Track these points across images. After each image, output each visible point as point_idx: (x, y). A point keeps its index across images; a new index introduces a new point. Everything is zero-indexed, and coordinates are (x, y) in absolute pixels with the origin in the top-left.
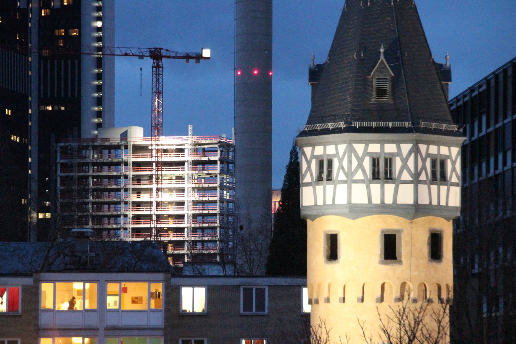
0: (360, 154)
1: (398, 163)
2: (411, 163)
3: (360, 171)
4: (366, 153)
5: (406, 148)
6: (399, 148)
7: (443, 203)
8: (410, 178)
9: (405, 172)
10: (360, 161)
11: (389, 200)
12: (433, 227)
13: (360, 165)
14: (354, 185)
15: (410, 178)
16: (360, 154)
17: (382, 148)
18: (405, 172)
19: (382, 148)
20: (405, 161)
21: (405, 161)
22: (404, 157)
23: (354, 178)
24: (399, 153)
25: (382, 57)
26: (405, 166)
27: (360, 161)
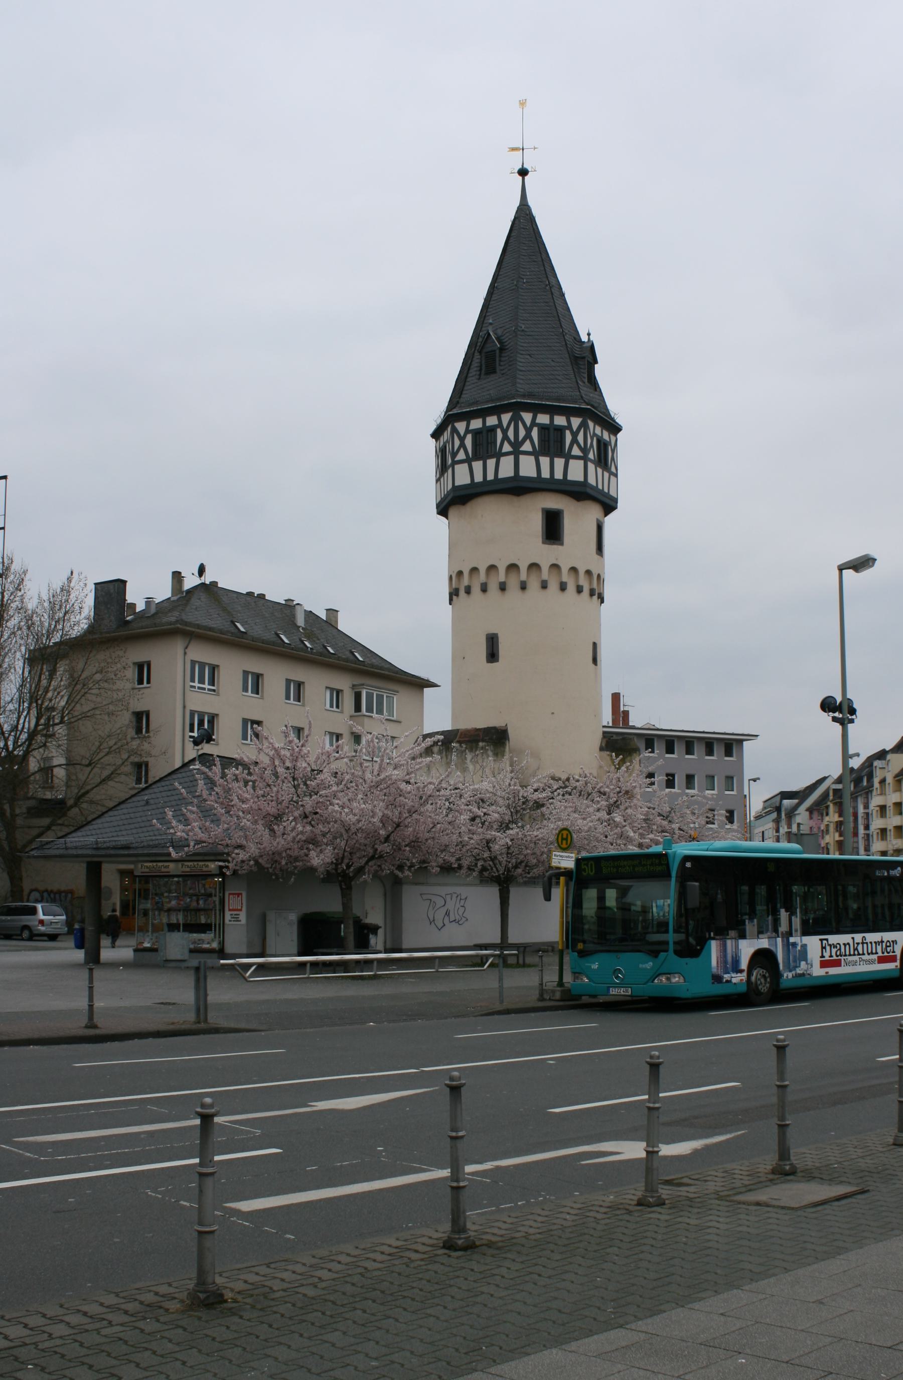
1: (499, 435)
3: (462, 451)
4: (467, 431)
5: (506, 418)
6: (500, 419)
7: (559, 475)
8: (511, 450)
9: (506, 444)
13: (462, 445)
15: (511, 450)
16: (462, 434)
17: (484, 422)
18: (506, 444)
19: (484, 422)
20: (505, 432)
21: (505, 432)
26: (505, 437)
27: (462, 439)
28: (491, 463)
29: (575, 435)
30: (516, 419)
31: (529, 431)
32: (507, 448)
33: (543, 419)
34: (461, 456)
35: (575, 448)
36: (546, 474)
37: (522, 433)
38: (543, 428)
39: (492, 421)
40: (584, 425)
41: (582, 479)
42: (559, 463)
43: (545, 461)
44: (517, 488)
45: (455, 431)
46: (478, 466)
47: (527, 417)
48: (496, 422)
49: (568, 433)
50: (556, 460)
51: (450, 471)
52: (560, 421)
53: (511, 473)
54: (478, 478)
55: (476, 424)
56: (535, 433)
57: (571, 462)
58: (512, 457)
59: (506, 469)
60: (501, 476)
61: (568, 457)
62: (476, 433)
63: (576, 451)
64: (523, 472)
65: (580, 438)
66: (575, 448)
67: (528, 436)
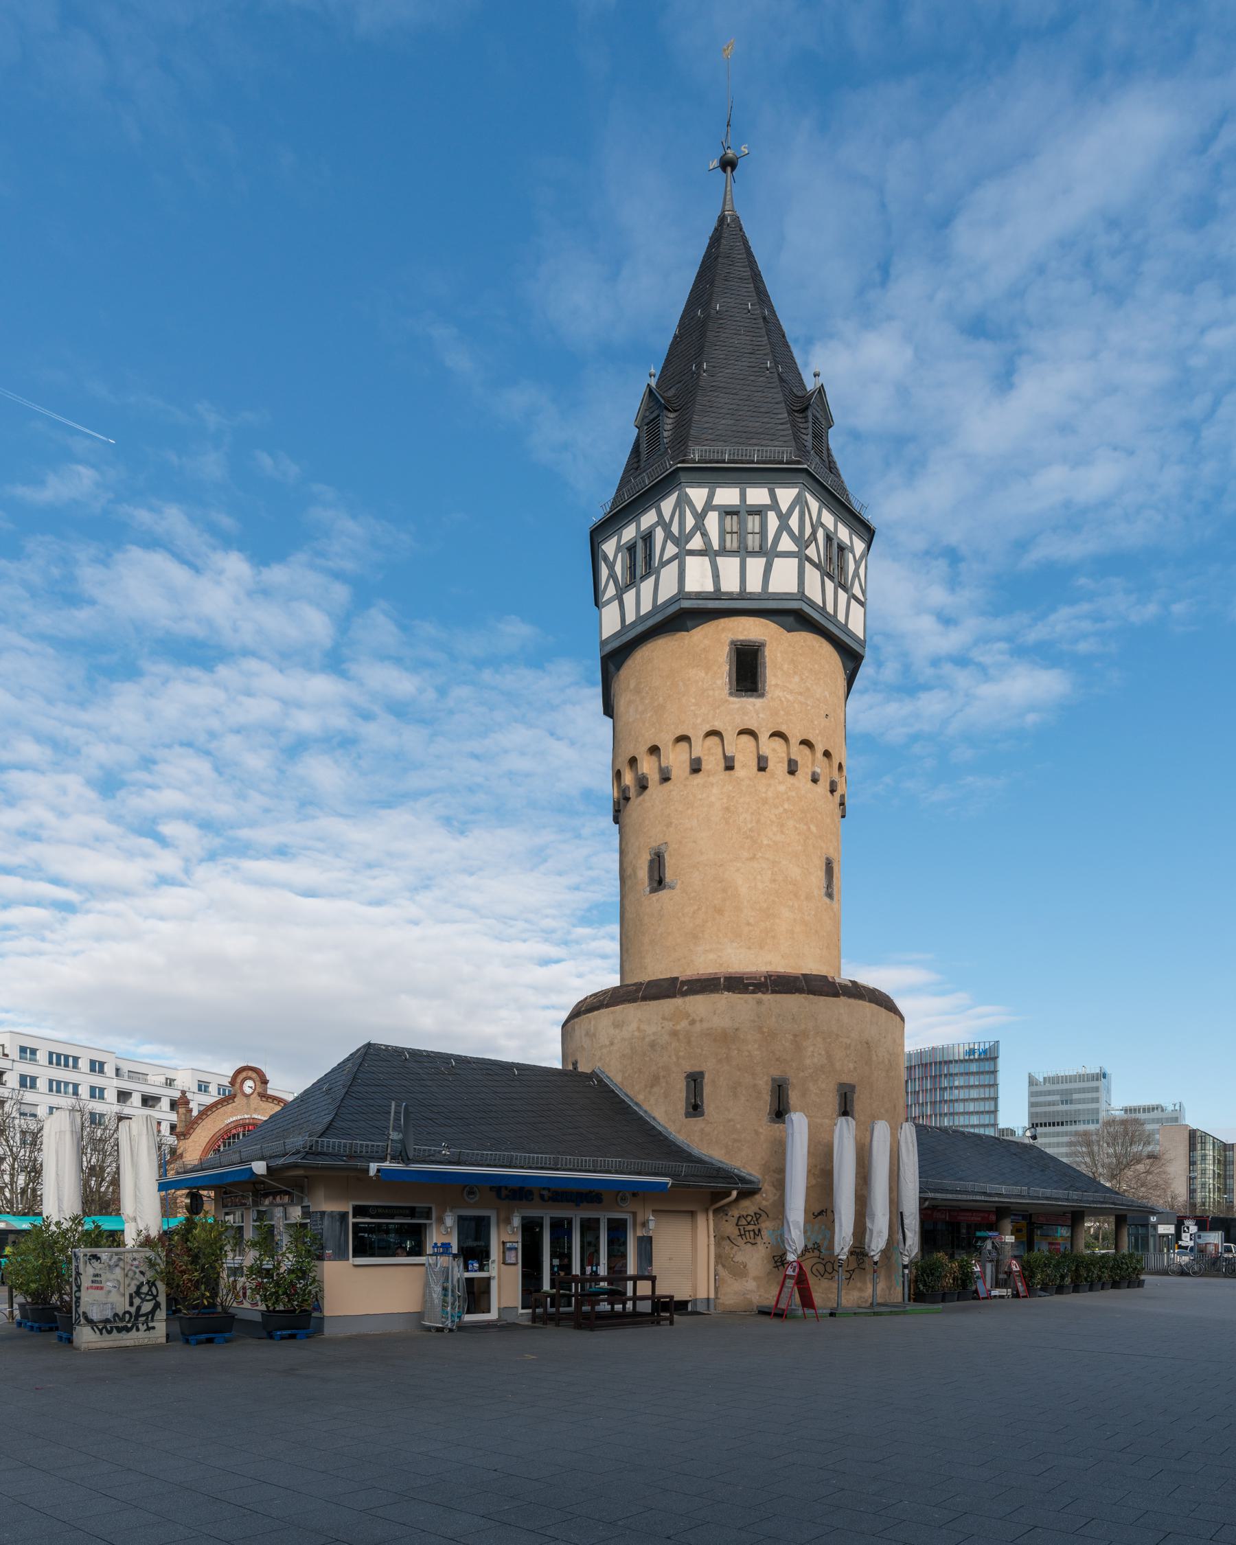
1: (773, 521)
2: (794, 522)
5: (786, 496)
8: (795, 548)
11: (754, 586)
13: (700, 527)
14: (689, 559)
15: (795, 548)
17: (743, 496)
20: (784, 518)
21: (784, 518)
23: (688, 547)
24: (775, 505)
26: (784, 526)
27: (700, 517)
28: (756, 566)
30: (799, 501)
32: (786, 544)
34: (696, 543)
39: (758, 496)
45: (684, 501)
48: (768, 501)
51: (669, 575)
53: (793, 588)
55: (727, 496)
56: (820, 535)
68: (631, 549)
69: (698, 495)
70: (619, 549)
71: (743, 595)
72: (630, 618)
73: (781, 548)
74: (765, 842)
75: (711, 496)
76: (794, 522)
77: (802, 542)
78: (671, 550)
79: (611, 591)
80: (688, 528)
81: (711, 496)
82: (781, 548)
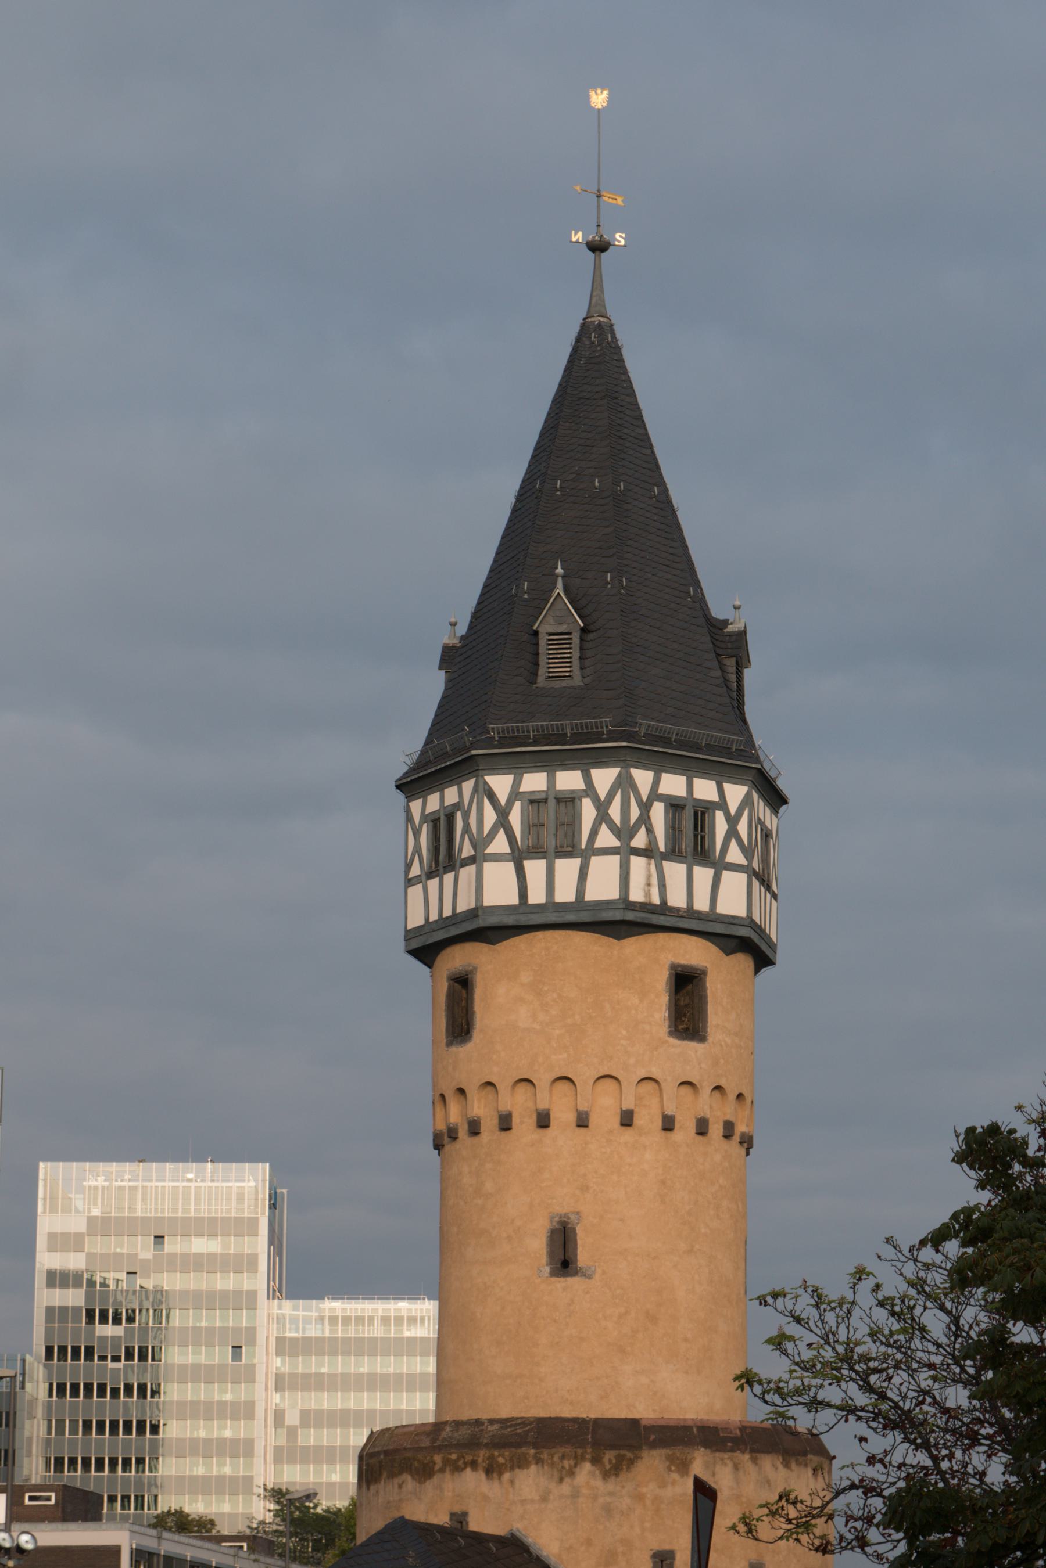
0: (503, 798)
1: (588, 811)
3: (501, 834)
4: (515, 794)
5: (604, 778)
7: (701, 904)
10: (503, 814)
11: (565, 894)
12: (683, 962)
16: (503, 799)
17: (551, 781)
19: (551, 781)
21: (602, 808)
22: (602, 797)
24: (590, 789)
25: (559, 589)
26: (603, 817)
28: (567, 869)
29: (732, 821)
30: (624, 784)
31: (645, 807)
32: (606, 838)
33: (673, 784)
35: (734, 848)
36: (677, 899)
37: (635, 812)
38: (675, 806)
39: (569, 780)
40: (747, 802)
41: (742, 913)
42: (703, 875)
43: (676, 871)
44: (622, 922)
46: (535, 868)
47: (643, 778)
48: (581, 785)
49: (719, 816)
50: (697, 870)
52: (705, 789)
54: (537, 896)
55: (535, 782)
56: (658, 813)
57: (726, 874)
58: (616, 859)
59: (603, 883)
60: (589, 897)
61: (720, 866)
62: (535, 801)
63: (735, 855)
64: (636, 895)
65: (743, 828)
66: (734, 848)
67: (645, 819)
68: (434, 821)
69: (501, 784)
70: (424, 818)
71: (549, 905)
72: (434, 917)
73: (599, 843)
74: (703, 1230)
75: (517, 783)
76: (615, 811)
77: (624, 832)
78: (467, 851)
79: (415, 871)
80: (487, 828)
81: (517, 783)
82: (599, 843)
